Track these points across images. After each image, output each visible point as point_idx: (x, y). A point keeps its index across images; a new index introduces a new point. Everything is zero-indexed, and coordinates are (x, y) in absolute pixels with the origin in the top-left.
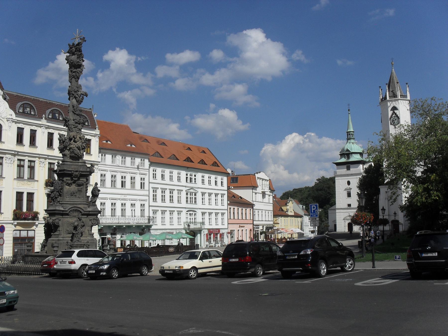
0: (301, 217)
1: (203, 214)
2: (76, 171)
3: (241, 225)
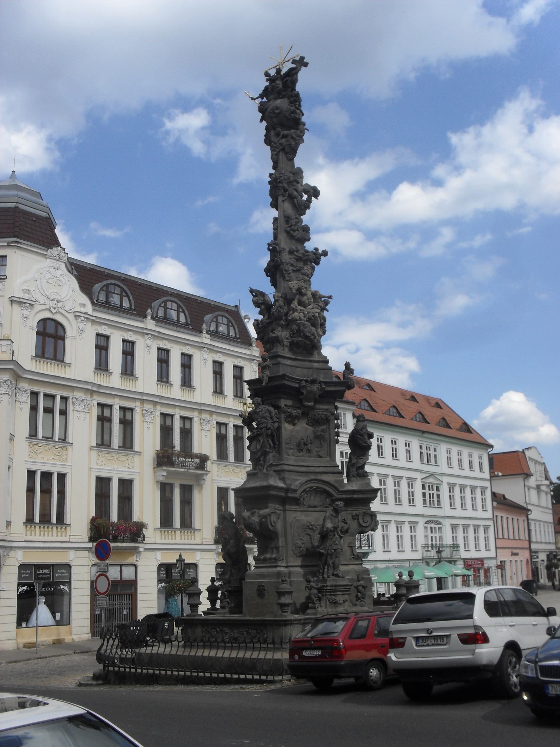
1: (454, 527)
2: (313, 382)
3: (515, 551)
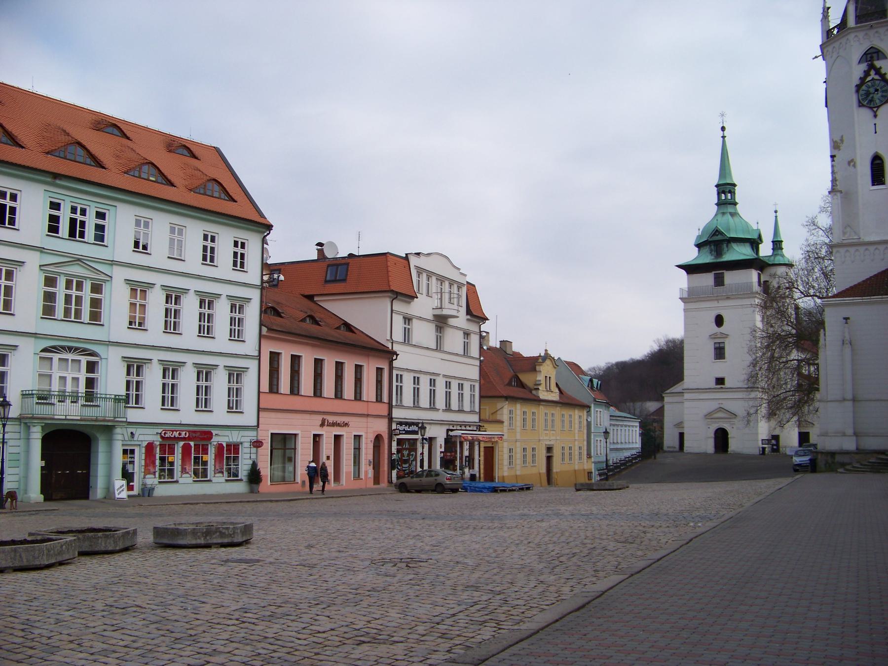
0: (586, 407)
3: (331, 419)
